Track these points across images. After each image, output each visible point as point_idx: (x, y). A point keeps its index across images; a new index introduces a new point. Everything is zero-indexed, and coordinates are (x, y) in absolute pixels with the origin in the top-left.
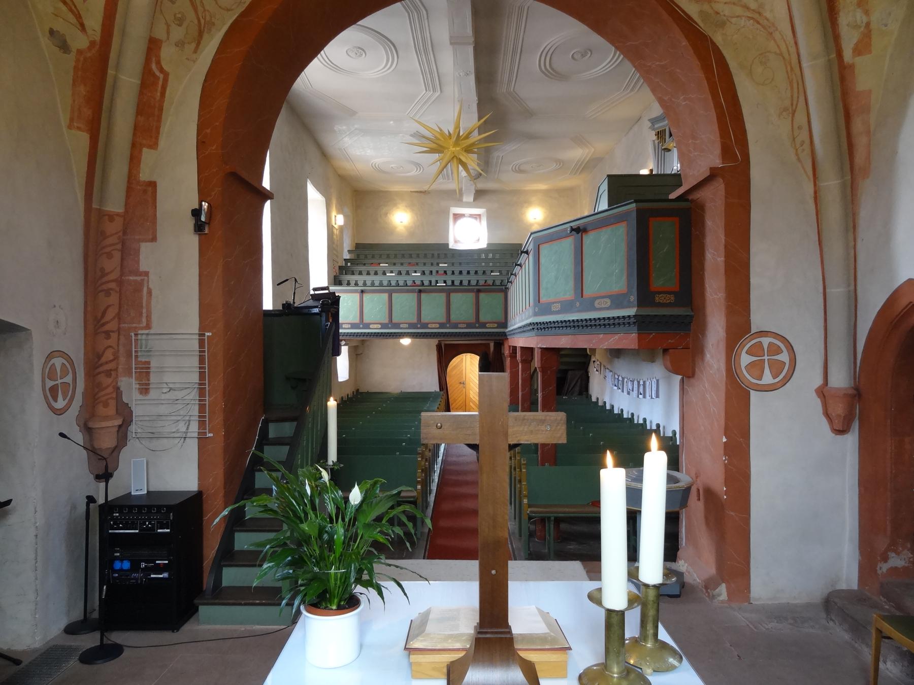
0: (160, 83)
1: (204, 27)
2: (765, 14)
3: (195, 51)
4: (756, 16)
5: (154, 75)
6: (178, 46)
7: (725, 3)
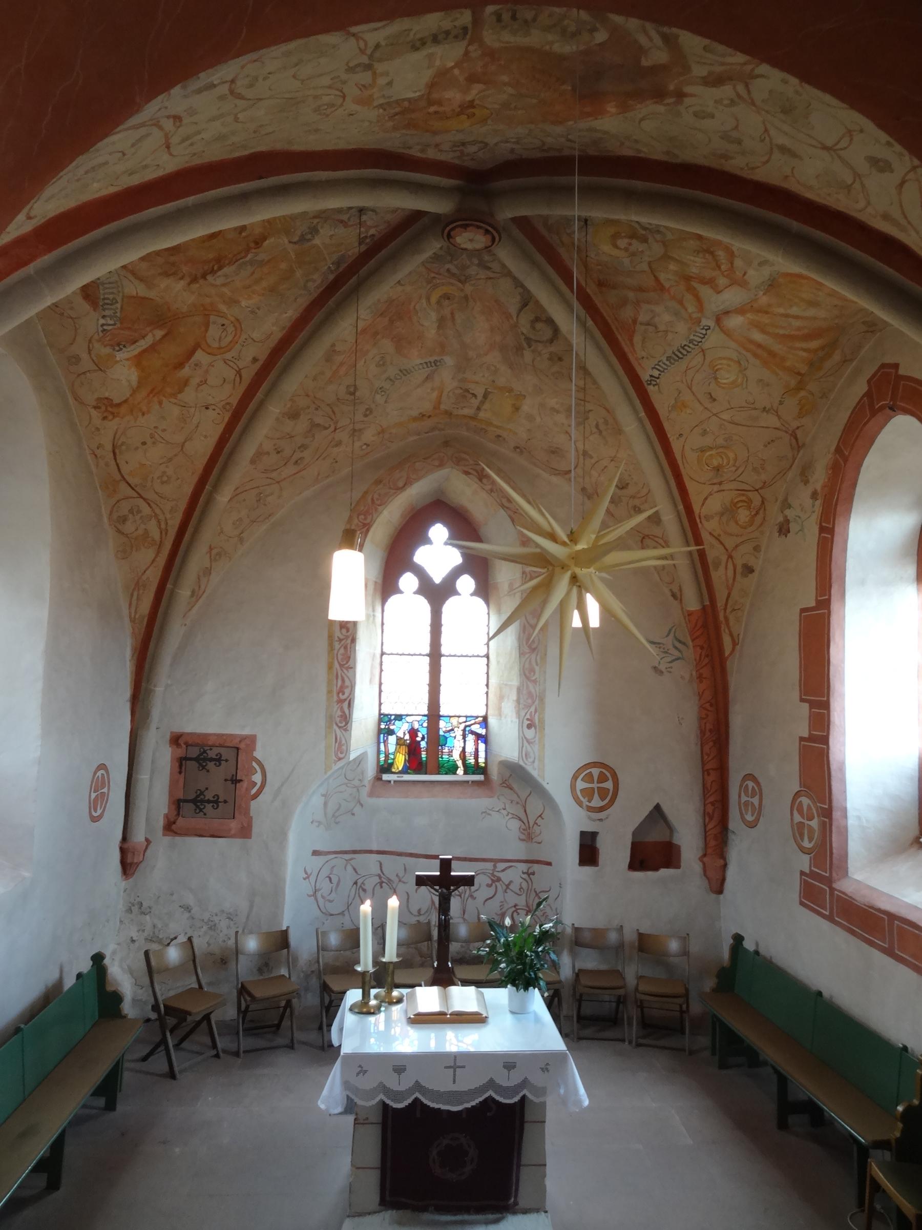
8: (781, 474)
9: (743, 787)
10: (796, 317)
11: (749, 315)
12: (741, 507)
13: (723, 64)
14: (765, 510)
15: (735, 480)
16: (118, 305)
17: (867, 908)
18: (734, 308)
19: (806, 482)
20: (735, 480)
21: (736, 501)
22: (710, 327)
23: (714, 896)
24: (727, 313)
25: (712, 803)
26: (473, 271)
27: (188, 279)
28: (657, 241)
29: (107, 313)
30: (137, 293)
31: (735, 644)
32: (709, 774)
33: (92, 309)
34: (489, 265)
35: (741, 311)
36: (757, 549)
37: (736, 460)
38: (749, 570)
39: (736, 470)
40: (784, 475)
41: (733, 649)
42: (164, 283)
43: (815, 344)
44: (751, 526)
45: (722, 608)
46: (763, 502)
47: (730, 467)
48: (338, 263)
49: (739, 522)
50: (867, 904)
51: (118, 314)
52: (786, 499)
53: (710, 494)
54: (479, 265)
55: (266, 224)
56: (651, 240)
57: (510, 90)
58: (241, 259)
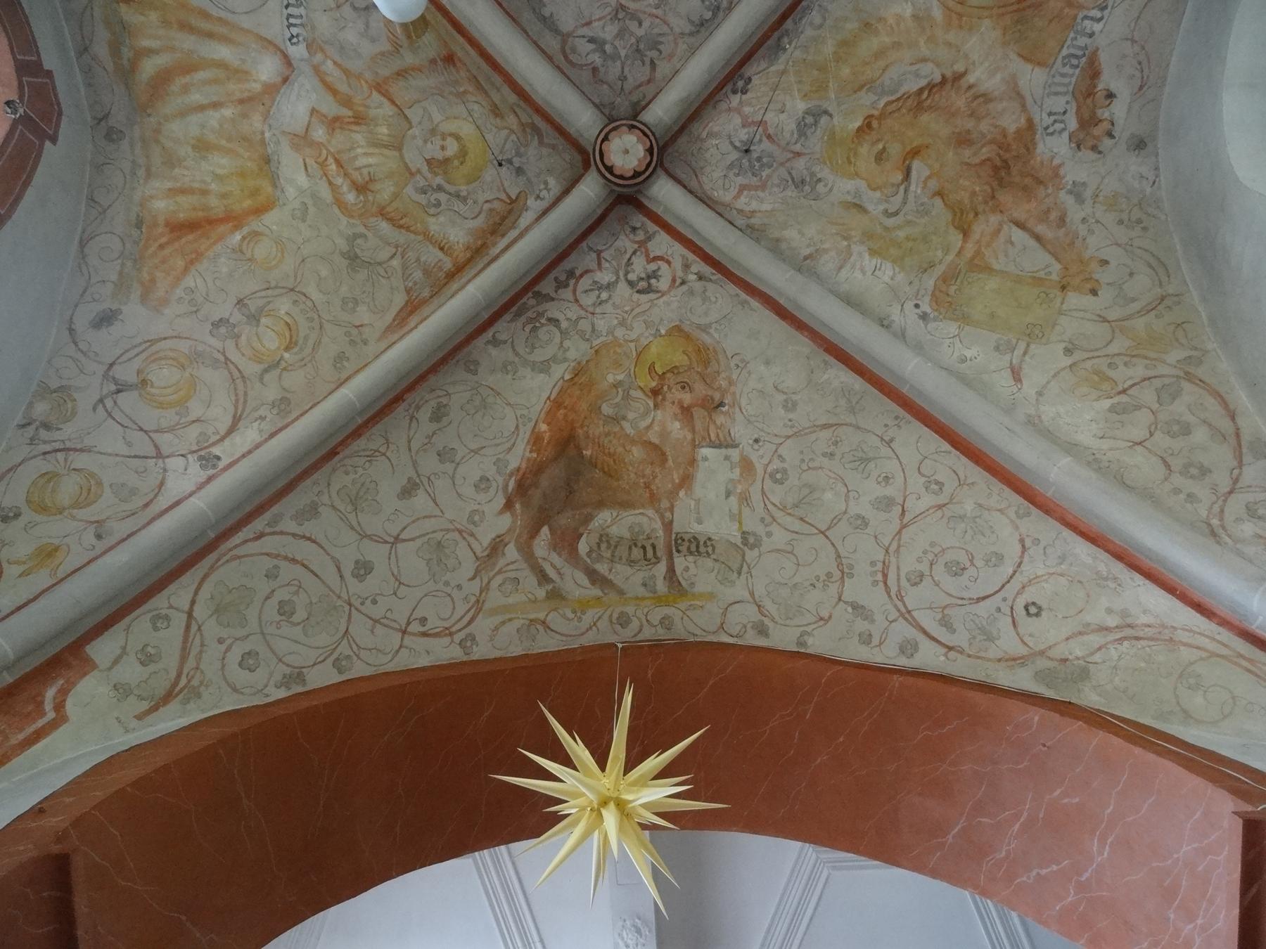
0: (40, 723)
1: (181, 691)
2: (1139, 622)
3: (139, 717)
4: (1128, 632)
5: (40, 705)
6: (117, 690)
7: (1067, 639)
10: (201, 108)
11: (257, 87)
13: (500, 572)
16: (1065, 52)
18: (282, 91)
22: (292, 44)
24: (285, 80)
26: (608, 32)
27: (964, 83)
28: (419, 171)
29: (1082, 41)
30: (1033, 70)
33: (1099, 53)
34: (592, 46)
35: (271, 90)
42: (993, 84)
43: (149, 67)
48: (779, 48)
51: (1072, 35)
54: (604, 42)
55: (853, 160)
56: (425, 169)
57: (629, 430)
58: (893, 102)
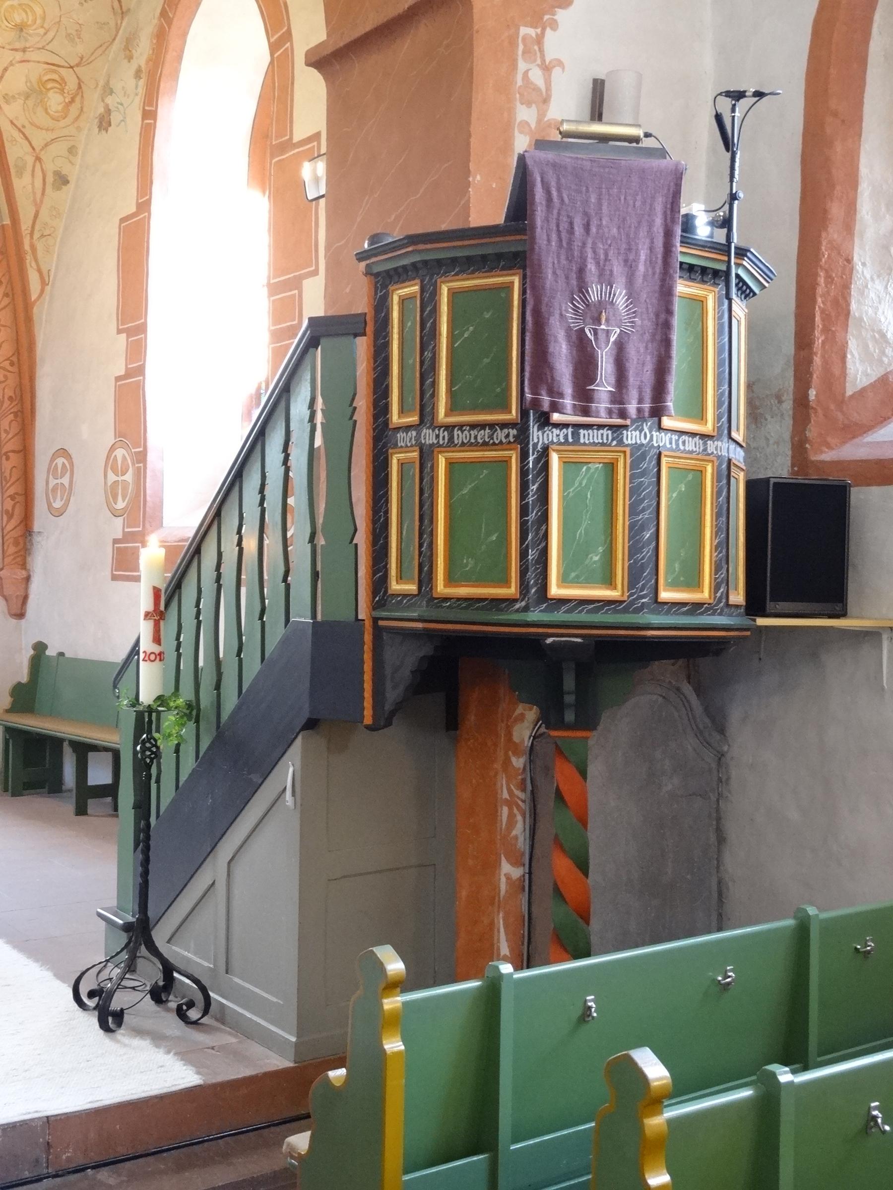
8: (100, 51)
9: (52, 470)
12: (52, 88)
14: (82, 96)
15: (43, 48)
17: (176, 544)
19: (130, 58)
20: (43, 48)
21: (46, 78)
23: (14, 621)
25: (12, 497)
31: (44, 283)
32: (8, 459)
36: (72, 150)
37: (44, 19)
38: (62, 180)
39: (45, 34)
40: (106, 49)
41: (42, 291)
44: (64, 119)
45: (27, 232)
46: (80, 87)
47: (35, 29)
49: (49, 111)
50: (177, 540)
52: (107, 83)
53: (11, 64)
